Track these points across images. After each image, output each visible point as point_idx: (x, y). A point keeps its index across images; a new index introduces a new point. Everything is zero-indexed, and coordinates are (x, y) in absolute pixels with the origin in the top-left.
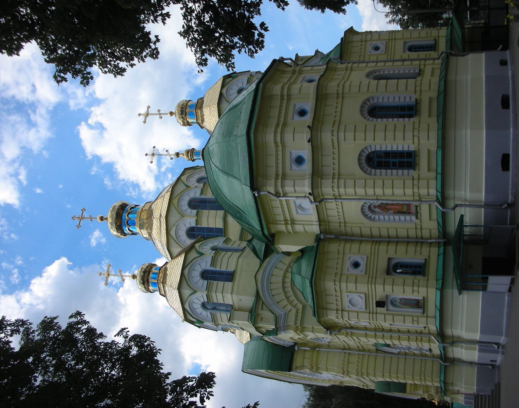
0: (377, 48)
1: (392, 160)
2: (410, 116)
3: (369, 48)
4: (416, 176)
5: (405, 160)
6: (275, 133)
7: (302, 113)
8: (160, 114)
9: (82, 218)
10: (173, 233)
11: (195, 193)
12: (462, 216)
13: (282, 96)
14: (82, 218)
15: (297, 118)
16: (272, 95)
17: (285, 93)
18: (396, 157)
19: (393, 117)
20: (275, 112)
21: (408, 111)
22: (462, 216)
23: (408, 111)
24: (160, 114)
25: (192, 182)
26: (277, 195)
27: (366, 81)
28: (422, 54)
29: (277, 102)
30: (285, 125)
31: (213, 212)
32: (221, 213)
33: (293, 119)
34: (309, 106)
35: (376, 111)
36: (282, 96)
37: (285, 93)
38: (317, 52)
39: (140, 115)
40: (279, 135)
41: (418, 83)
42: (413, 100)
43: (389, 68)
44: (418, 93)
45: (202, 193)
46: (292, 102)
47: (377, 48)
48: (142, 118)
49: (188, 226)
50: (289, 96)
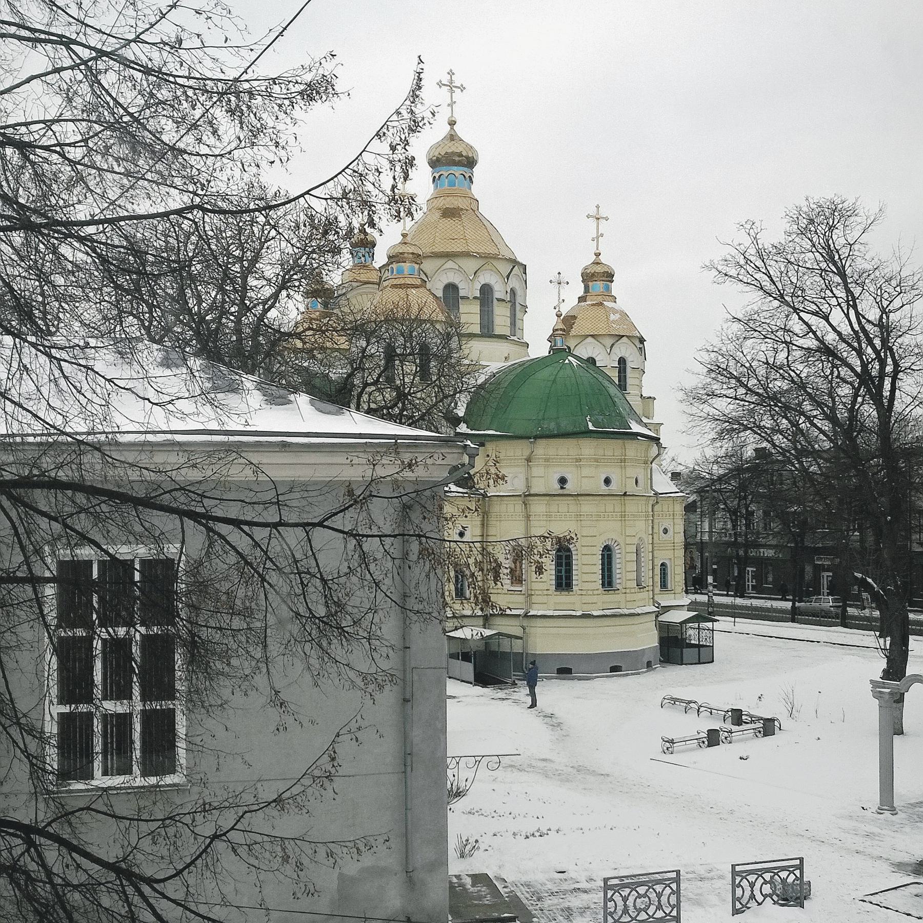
0: (666, 531)
1: (563, 569)
2: (603, 585)
3: (667, 524)
4: (549, 592)
5: (564, 582)
8: (598, 238)
9: (451, 86)
10: (450, 264)
11: (499, 291)
12: (521, 638)
14: (451, 86)
18: (566, 572)
19: (603, 569)
21: (608, 581)
22: (521, 638)
23: (608, 581)
24: (598, 238)
25: (513, 283)
26: (529, 460)
27: (635, 541)
28: (658, 578)
31: (477, 318)
32: (476, 329)
34: (614, 487)
35: (607, 554)
39: (598, 207)
41: (633, 591)
42: (618, 586)
43: (646, 556)
44: (624, 591)
45: (498, 300)
47: (666, 531)
48: (593, 211)
49: (460, 286)
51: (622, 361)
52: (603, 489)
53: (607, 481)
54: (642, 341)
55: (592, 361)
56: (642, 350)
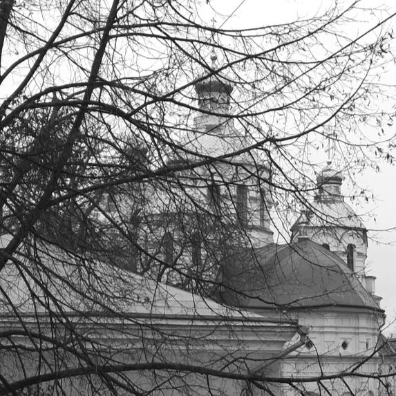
6: (331, 327)
7: (345, 345)
8: (329, 150)
13: (358, 328)
15: (342, 341)
16: (358, 319)
17: (360, 331)
20: (346, 323)
29: (353, 323)
30: (337, 333)
33: (341, 339)
34: (350, 351)
36: (358, 328)
37: (360, 331)
38: (384, 311)
40: (330, 330)
46: (351, 336)
50: (358, 333)
51: (351, 248)
52: (342, 352)
53: (345, 345)
54: (365, 231)
55: (326, 246)
56: (365, 241)
